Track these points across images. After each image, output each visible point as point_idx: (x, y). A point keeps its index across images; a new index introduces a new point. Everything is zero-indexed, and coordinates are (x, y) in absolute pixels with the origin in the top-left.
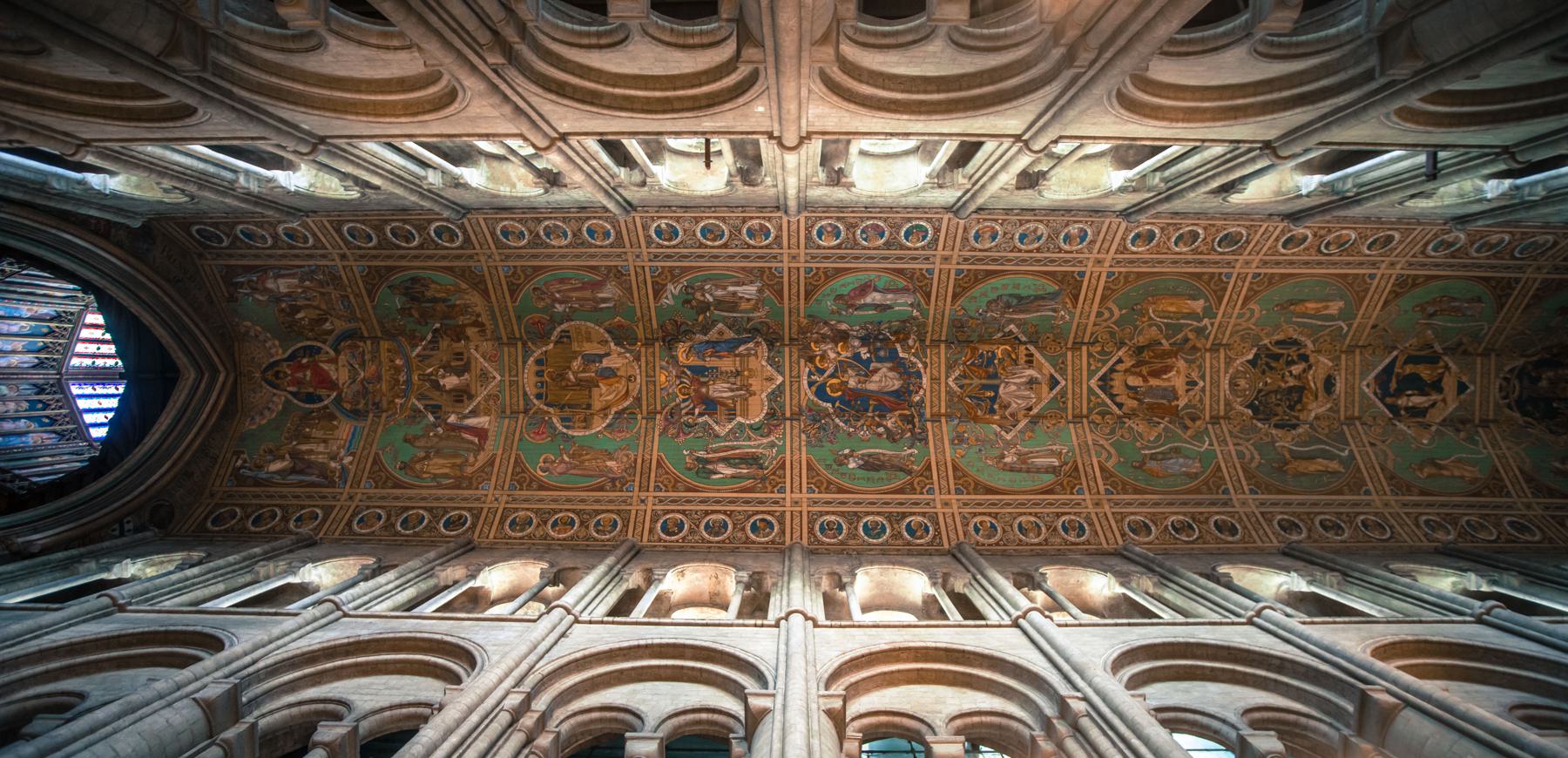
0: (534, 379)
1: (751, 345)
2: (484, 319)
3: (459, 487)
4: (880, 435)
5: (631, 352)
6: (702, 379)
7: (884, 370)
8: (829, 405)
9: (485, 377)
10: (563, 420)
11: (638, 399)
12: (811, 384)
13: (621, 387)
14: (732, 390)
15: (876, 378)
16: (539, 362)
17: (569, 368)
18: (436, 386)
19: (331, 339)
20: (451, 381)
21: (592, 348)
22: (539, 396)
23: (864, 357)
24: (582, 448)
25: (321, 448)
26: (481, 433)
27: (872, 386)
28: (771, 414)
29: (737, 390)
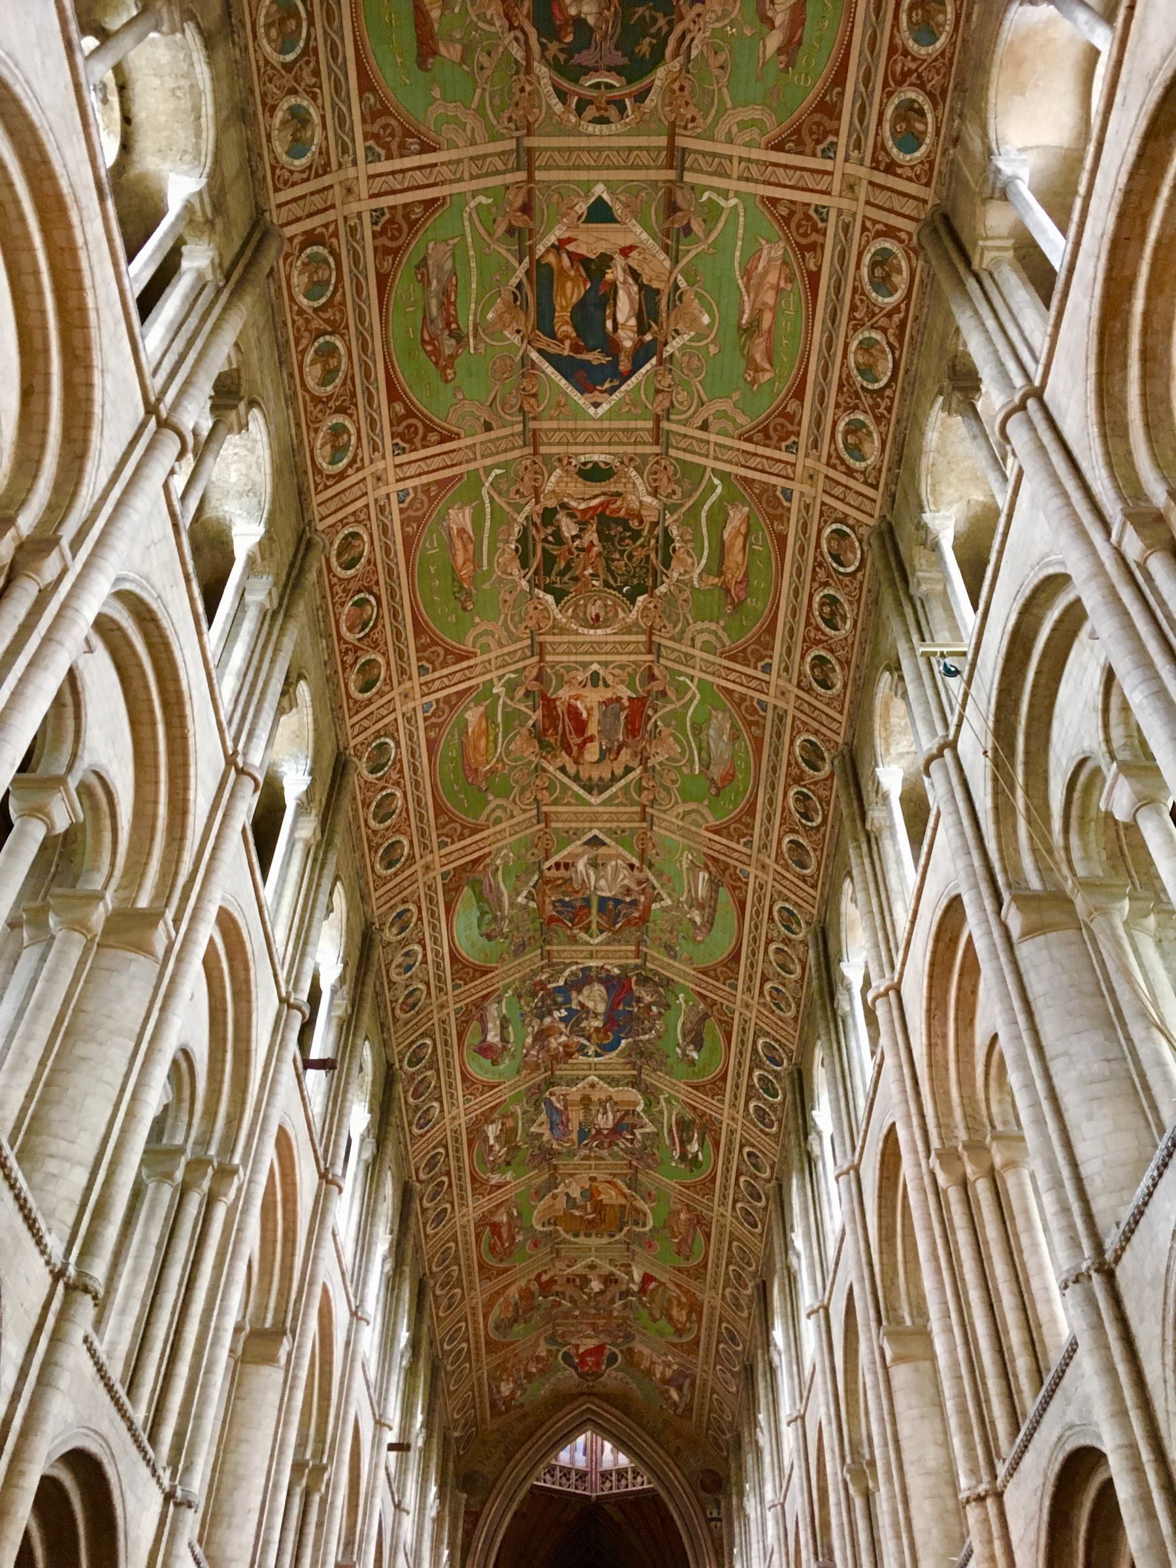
0: (593, 1238)
1: (553, 1099)
2: (533, 1276)
3: (700, 1314)
4: (660, 1013)
5: (563, 1180)
6: (593, 1132)
7: (580, 998)
8: (623, 1042)
9: (592, 1267)
10: (636, 1223)
11: (615, 1175)
12: (597, 1055)
13: (601, 1187)
14: (605, 1113)
15: (590, 1005)
16: (577, 1235)
17: (581, 1217)
18: (602, 1292)
19: (554, 1348)
20: (596, 1286)
21: (561, 1203)
22: (612, 1236)
23: (564, 1013)
24: (664, 1227)
25: (658, 1370)
26: (647, 1278)
27: (601, 1008)
28: (634, 1085)
29: (605, 1108)
